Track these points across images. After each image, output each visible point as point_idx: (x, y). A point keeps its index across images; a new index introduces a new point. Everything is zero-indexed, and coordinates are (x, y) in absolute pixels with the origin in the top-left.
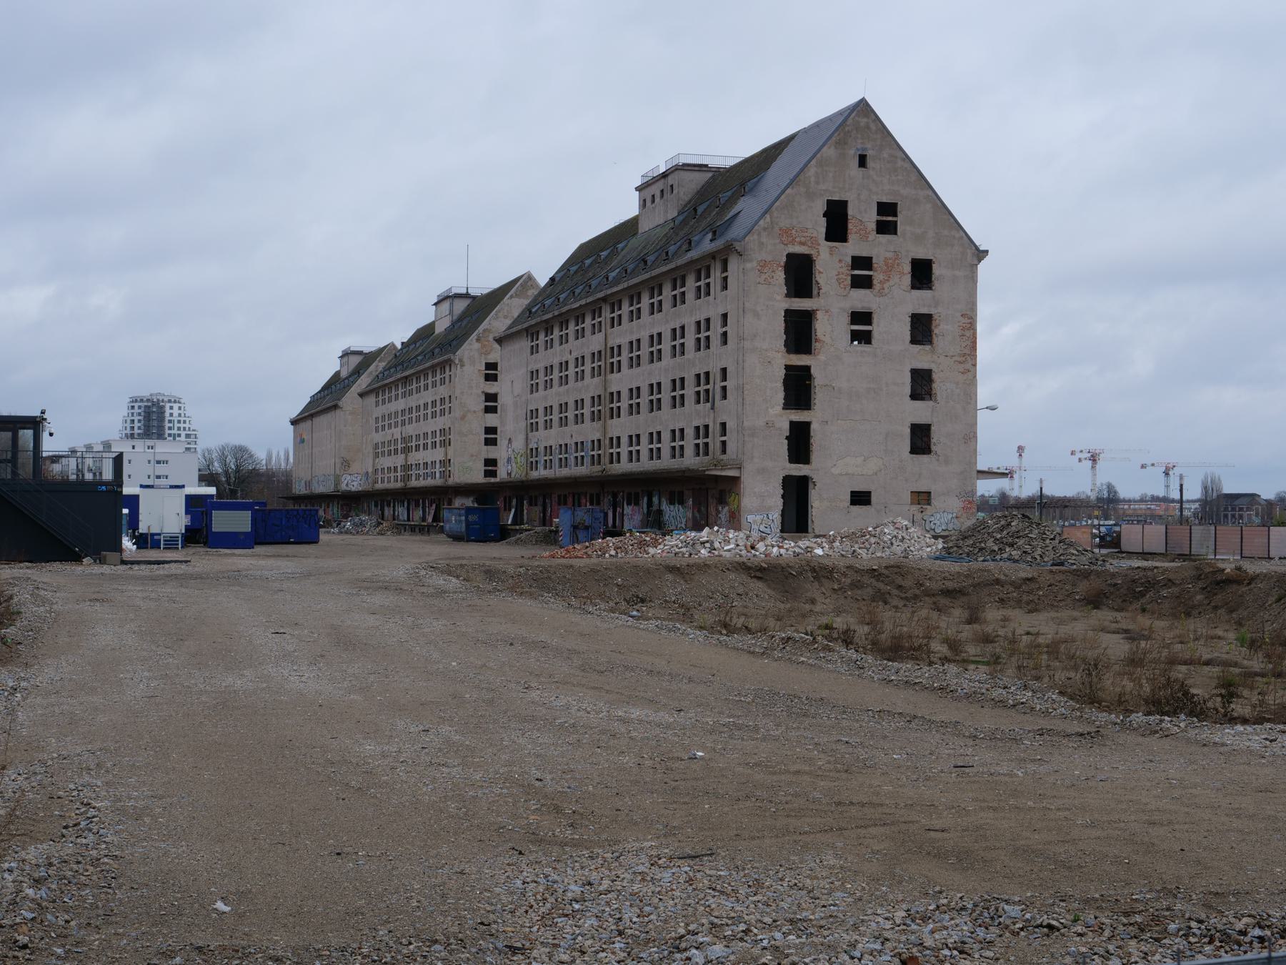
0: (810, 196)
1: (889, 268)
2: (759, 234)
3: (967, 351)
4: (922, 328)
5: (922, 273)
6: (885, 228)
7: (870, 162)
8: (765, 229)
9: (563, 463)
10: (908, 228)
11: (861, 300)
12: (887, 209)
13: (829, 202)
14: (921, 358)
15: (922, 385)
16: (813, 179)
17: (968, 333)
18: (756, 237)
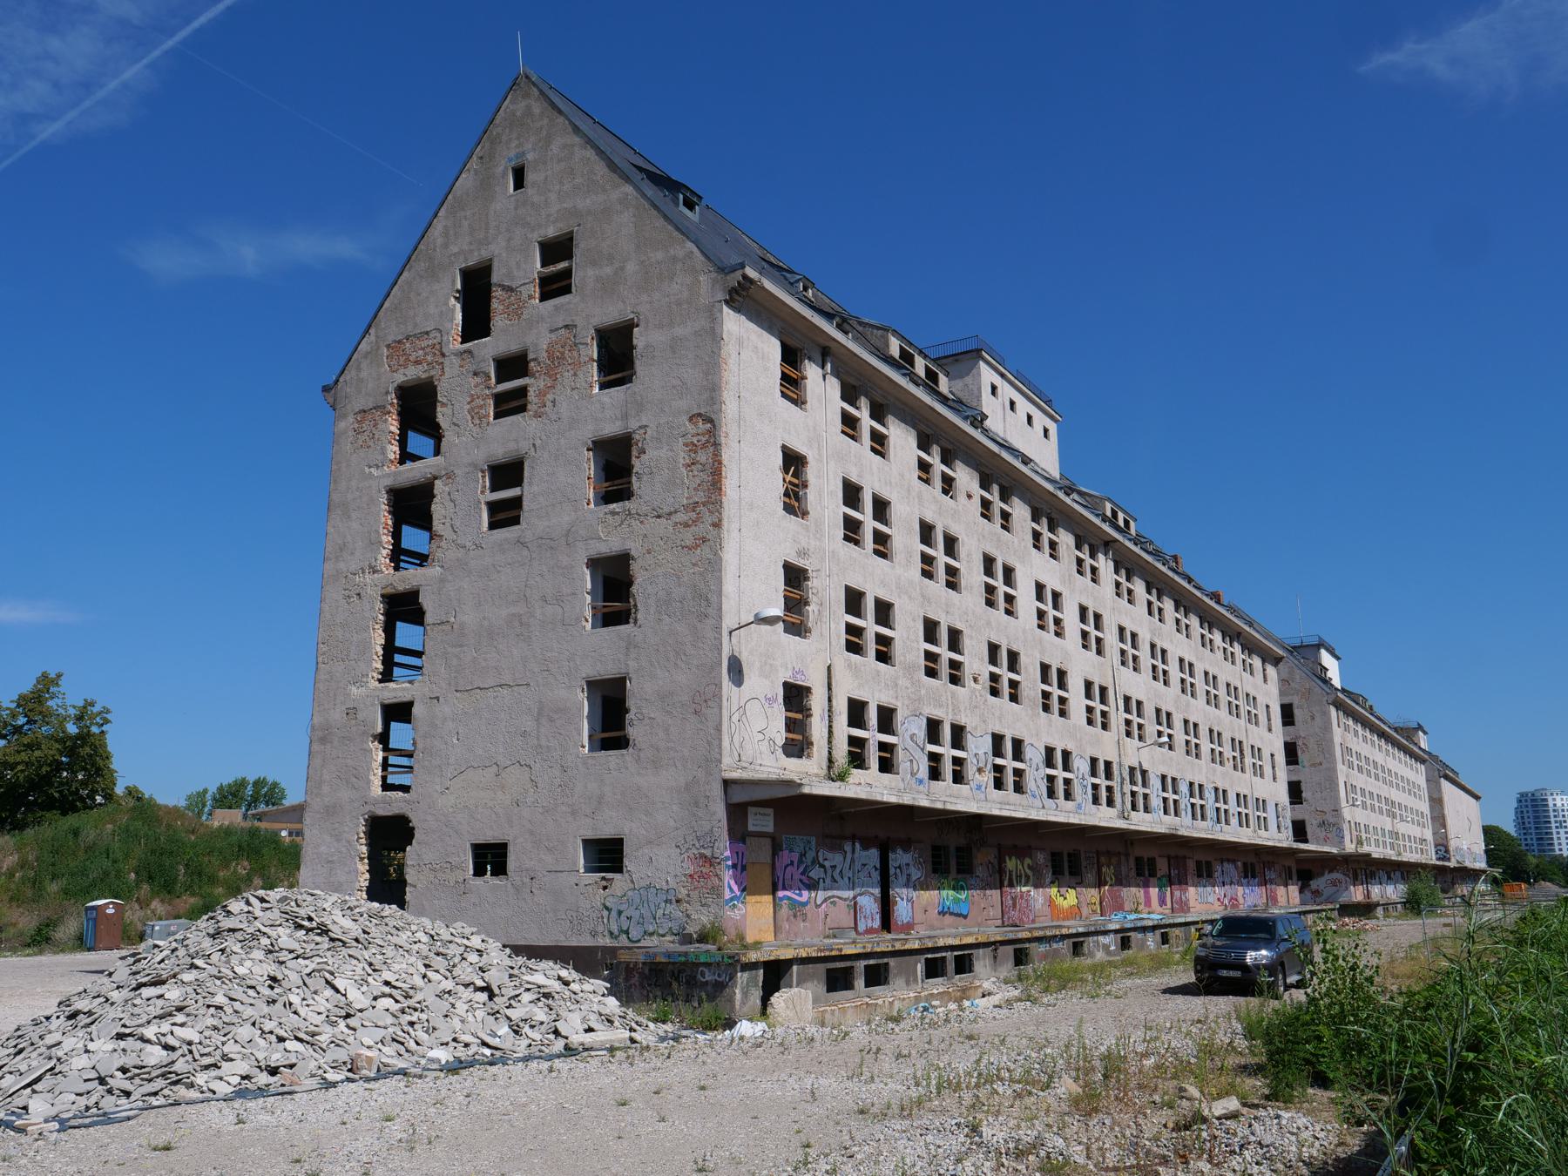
0: (433, 273)
1: (555, 360)
2: (359, 369)
3: (700, 497)
4: (615, 466)
5: (617, 356)
6: (554, 286)
7: (530, 177)
8: (368, 353)
9: (1198, 813)
10: (591, 272)
11: (504, 438)
12: (557, 249)
13: (467, 274)
14: (610, 532)
15: (614, 587)
17: (702, 457)
18: (353, 373)
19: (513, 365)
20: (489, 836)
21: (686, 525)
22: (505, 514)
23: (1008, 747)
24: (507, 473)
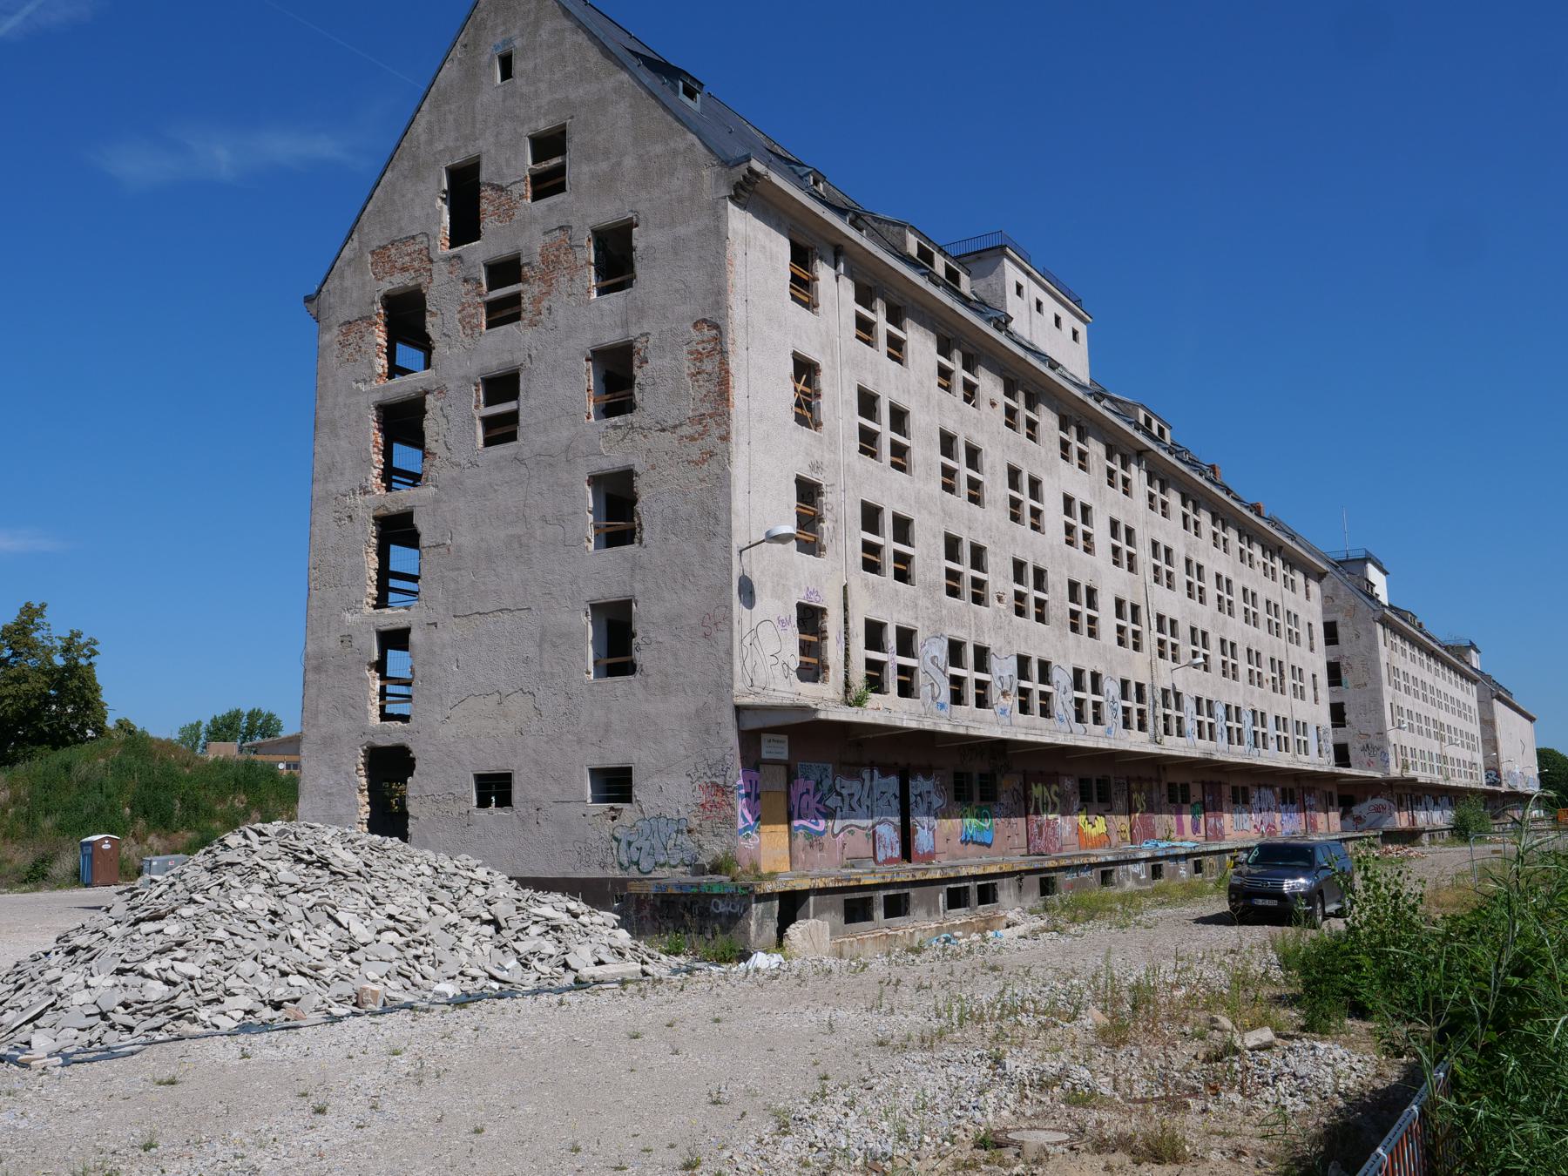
1: (551, 263)
2: (342, 277)
3: (706, 408)
4: (616, 376)
5: (615, 259)
6: (547, 184)
7: (518, 66)
9: (1235, 737)
10: (585, 169)
11: (499, 348)
12: (549, 144)
14: (612, 447)
15: (618, 506)
16: (423, 138)
17: (708, 366)
18: (337, 282)
19: (505, 271)
20: (493, 766)
21: (692, 439)
22: (501, 430)
23: (969, 655)
24: (502, 386)
